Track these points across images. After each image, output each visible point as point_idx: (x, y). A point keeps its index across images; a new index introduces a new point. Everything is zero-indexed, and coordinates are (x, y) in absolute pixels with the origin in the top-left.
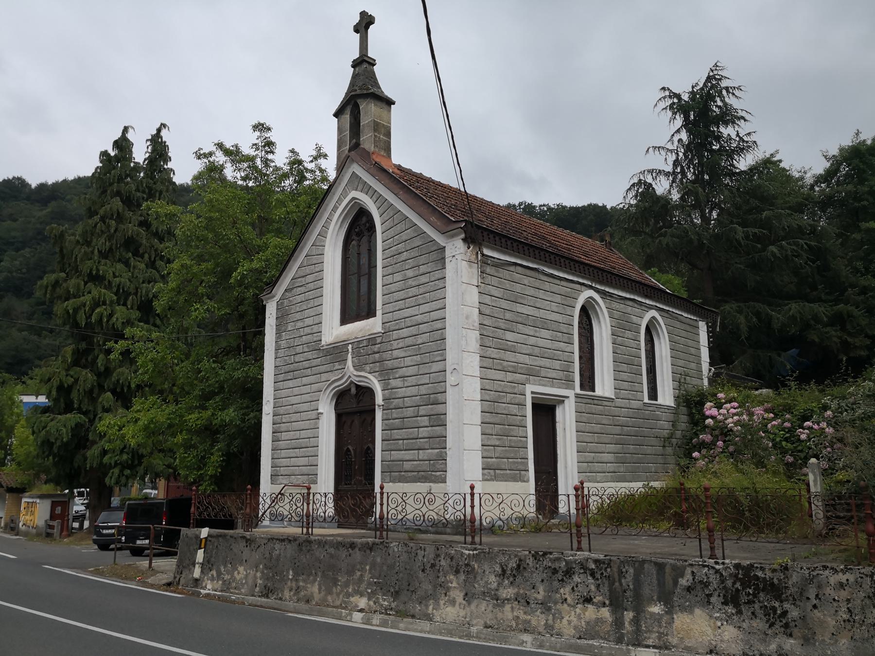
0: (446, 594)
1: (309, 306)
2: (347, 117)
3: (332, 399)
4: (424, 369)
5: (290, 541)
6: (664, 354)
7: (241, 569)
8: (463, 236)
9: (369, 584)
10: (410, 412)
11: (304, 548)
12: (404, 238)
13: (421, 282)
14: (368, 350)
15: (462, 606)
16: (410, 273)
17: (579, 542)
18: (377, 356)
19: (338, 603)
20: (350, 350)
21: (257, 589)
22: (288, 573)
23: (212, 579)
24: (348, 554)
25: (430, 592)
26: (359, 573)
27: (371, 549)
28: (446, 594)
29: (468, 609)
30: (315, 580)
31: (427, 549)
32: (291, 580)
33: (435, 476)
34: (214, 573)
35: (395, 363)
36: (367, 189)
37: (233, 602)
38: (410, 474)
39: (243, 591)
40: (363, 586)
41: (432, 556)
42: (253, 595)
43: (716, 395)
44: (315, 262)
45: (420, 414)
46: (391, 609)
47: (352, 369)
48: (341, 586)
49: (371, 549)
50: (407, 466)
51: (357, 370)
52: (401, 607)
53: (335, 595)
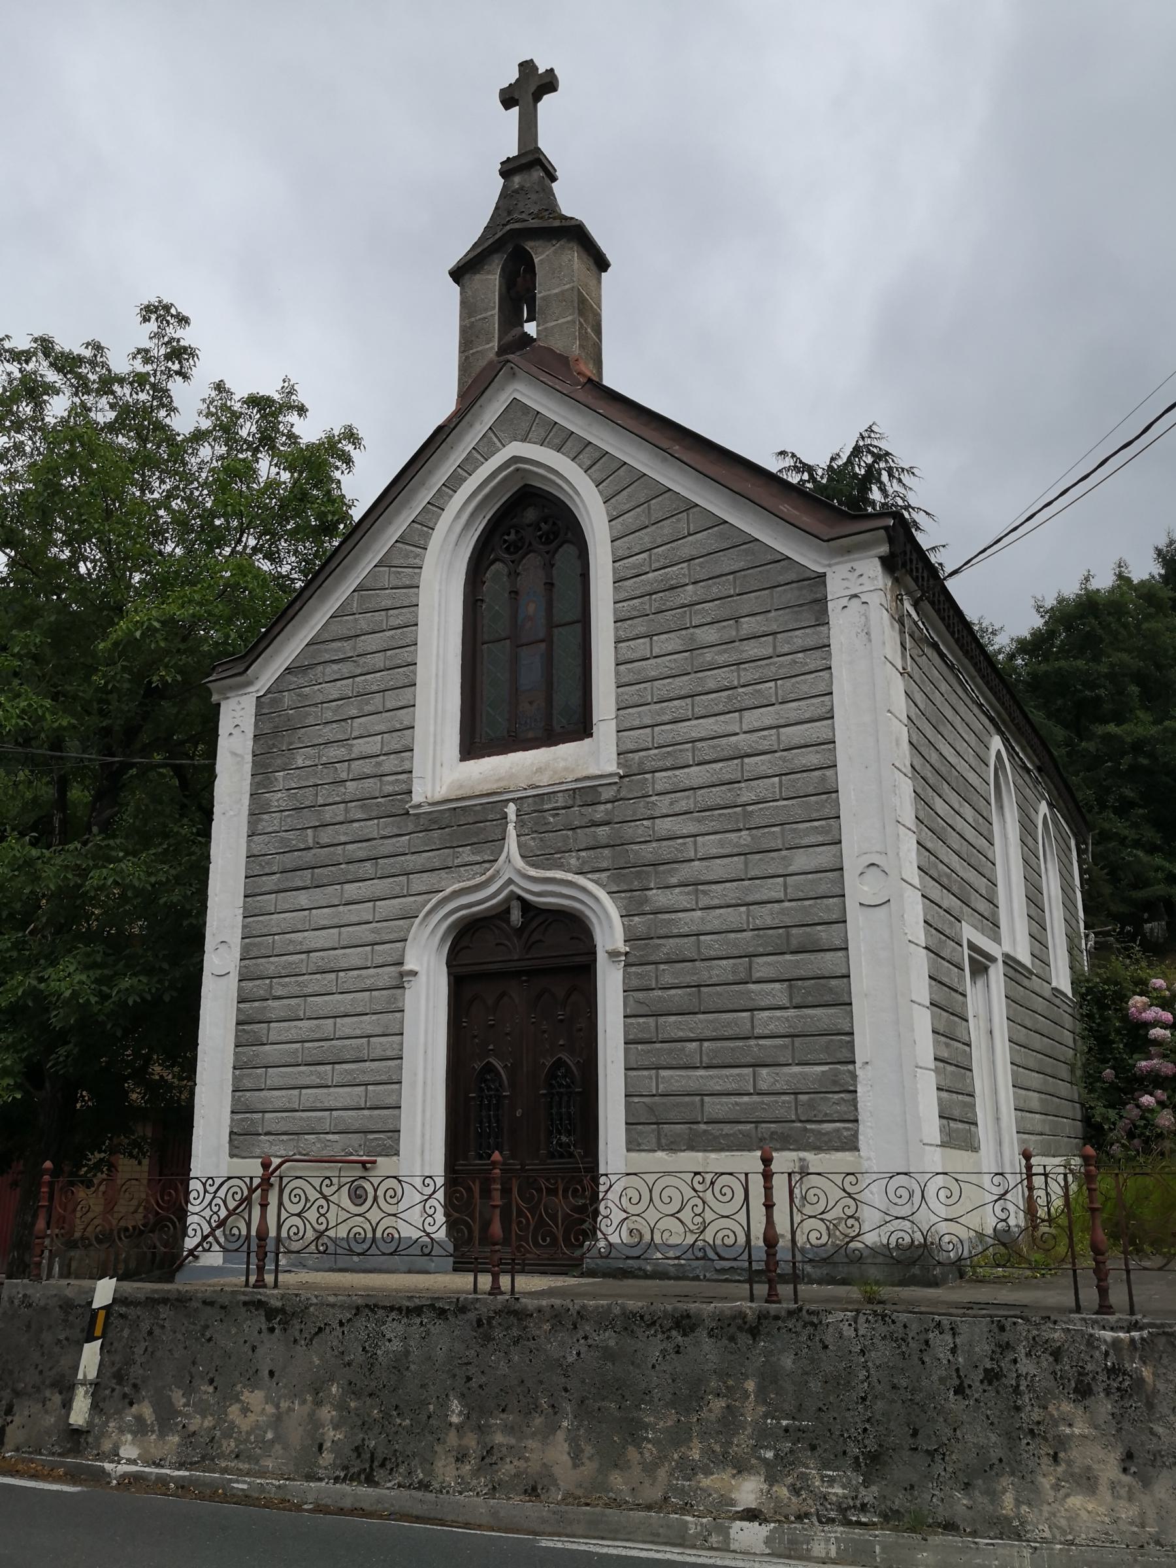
0: (1055, 1458)
1: (368, 708)
2: (491, 280)
3: (443, 940)
4: (758, 865)
5: (442, 1313)
6: (1053, 893)
7: (255, 1398)
8: (884, 549)
9: (763, 1436)
10: (722, 970)
11: (498, 1333)
12: (686, 552)
13: (745, 656)
14: (558, 819)
15: (1123, 1492)
16: (709, 635)
17: (1103, 1292)
18: (602, 831)
19: (656, 1494)
20: (512, 816)
21: (327, 1458)
22: (444, 1405)
23: (140, 1429)
24: (670, 1346)
25: (995, 1454)
26: (719, 1404)
27: (754, 1332)
28: (1055, 1458)
29: (1146, 1499)
30: (554, 1428)
31: (963, 1329)
32: (459, 1428)
33: (819, 1133)
34: (146, 1411)
35: (666, 850)
36: (561, 439)
37: (245, 1499)
38: (727, 1129)
39: (269, 1463)
40: (742, 1442)
41: (983, 1348)
42: (311, 1477)
43: (1144, 982)
44: (388, 603)
45: (756, 975)
46: (863, 1508)
47: (519, 863)
48: (656, 1442)
49: (754, 1332)
50: (716, 1107)
51: (533, 865)
52: (899, 1501)
53: (637, 1470)
